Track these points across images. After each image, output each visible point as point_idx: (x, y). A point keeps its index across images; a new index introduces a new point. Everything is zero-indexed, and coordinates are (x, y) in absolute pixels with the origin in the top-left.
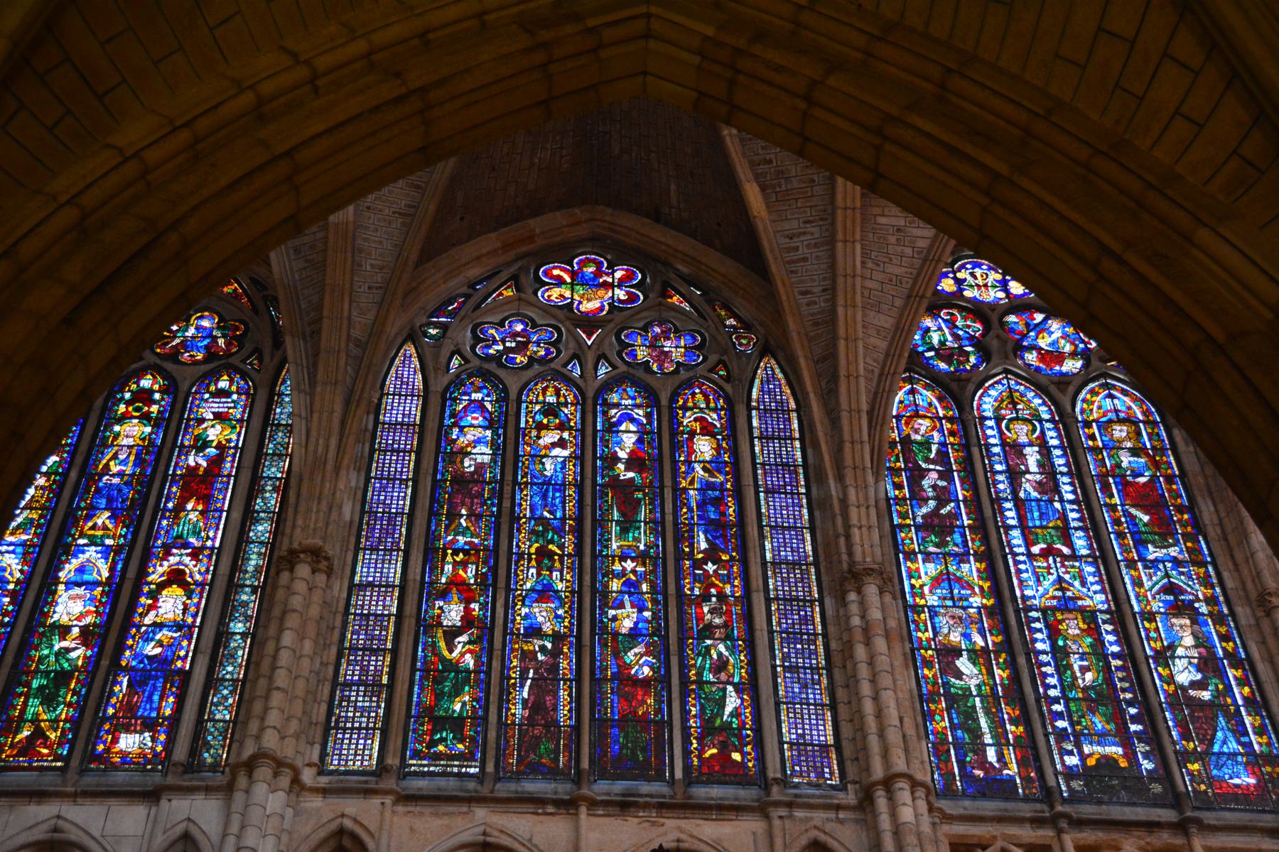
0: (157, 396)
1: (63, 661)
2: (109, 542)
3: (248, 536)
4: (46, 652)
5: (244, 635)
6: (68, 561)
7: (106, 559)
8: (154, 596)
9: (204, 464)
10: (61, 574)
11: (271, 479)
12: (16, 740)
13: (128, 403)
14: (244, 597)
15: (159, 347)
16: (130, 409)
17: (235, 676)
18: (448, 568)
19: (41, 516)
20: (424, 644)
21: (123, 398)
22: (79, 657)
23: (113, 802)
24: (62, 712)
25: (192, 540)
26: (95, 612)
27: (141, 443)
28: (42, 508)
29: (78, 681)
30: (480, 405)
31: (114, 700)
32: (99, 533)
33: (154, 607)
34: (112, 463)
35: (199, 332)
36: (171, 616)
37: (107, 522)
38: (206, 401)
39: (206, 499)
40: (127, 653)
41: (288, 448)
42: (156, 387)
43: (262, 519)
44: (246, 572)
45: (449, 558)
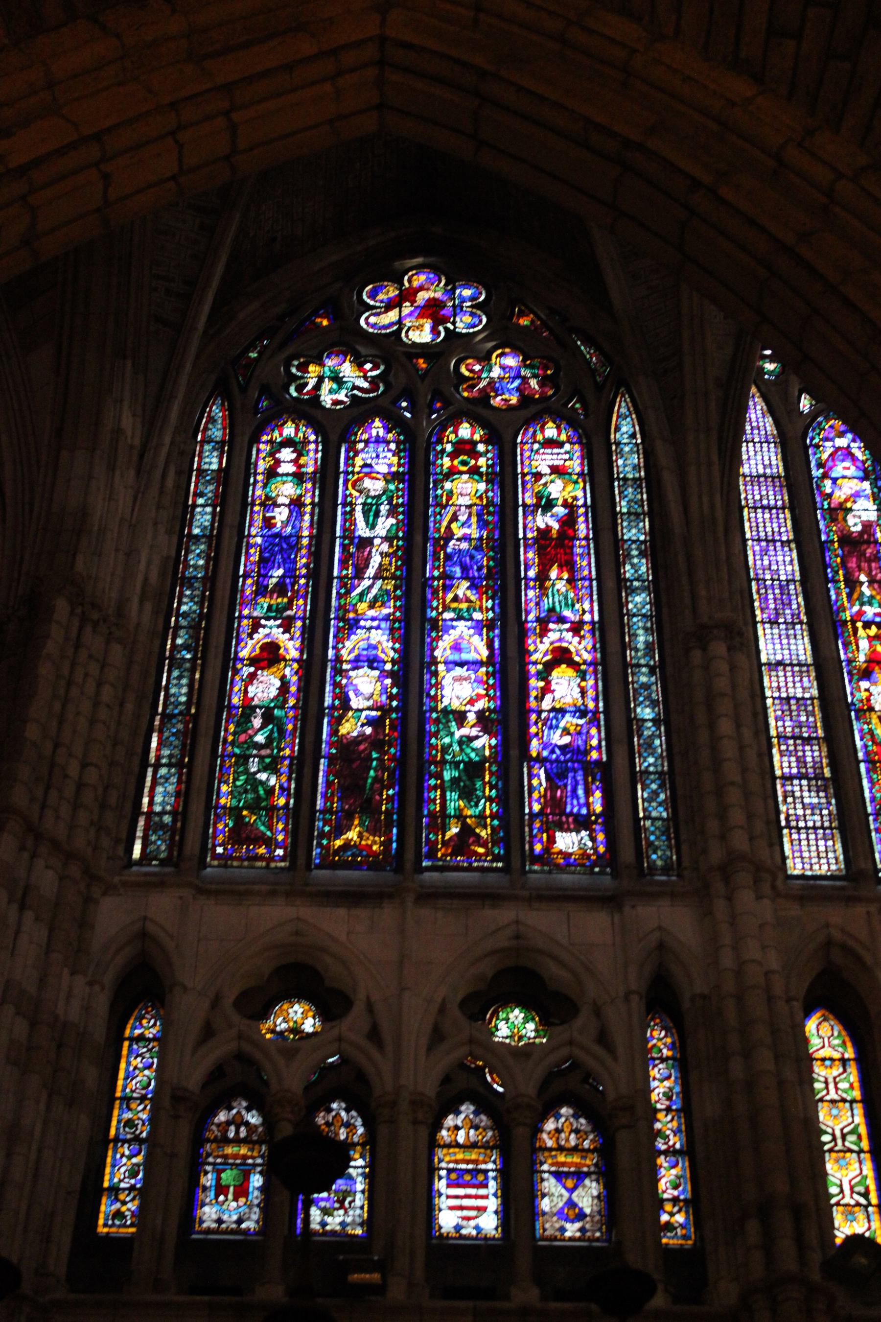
0: (481, 448)
1: (468, 751)
2: (477, 616)
3: (627, 609)
4: (447, 740)
5: (656, 721)
6: (438, 638)
7: (481, 635)
9: (556, 526)
10: (436, 653)
11: (634, 542)
12: (447, 838)
13: (453, 456)
14: (644, 679)
15: (464, 390)
16: (456, 462)
17: (659, 769)
18: (864, 644)
19: (396, 588)
20: (861, 731)
21: (443, 451)
22: (484, 746)
24: (490, 808)
25: (567, 613)
26: (487, 695)
27: (478, 502)
28: (394, 577)
29: (491, 774)
30: (848, 453)
31: (536, 795)
32: (464, 606)
33: (547, 690)
34: (454, 526)
35: (505, 373)
36: (569, 700)
37: (468, 593)
38: (537, 452)
39: (569, 565)
40: (535, 743)
41: (643, 506)
42: (477, 437)
43: (637, 588)
44: (637, 650)
45: (861, 632)
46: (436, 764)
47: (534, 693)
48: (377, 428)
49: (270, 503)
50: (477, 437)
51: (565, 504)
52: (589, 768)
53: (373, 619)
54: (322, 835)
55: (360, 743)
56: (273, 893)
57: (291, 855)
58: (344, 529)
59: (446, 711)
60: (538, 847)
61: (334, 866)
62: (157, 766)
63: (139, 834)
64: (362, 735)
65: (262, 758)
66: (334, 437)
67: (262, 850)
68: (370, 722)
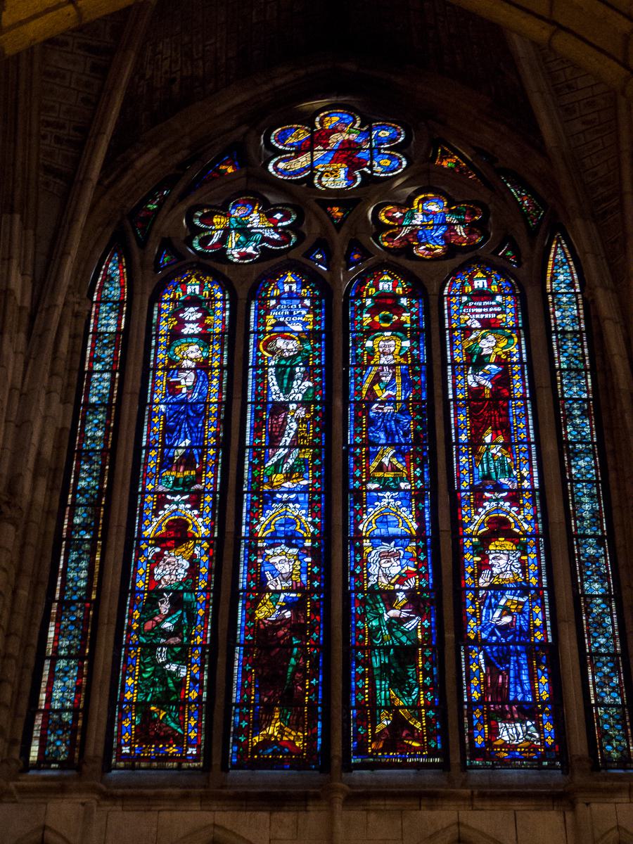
0: (404, 301)
1: (399, 634)
3: (571, 475)
4: (375, 623)
7: (409, 506)
8: (481, 548)
10: (361, 527)
11: (576, 400)
12: (377, 731)
13: (373, 311)
14: (591, 551)
15: (385, 239)
16: (377, 318)
17: (612, 650)
19: (314, 456)
21: (363, 306)
22: (416, 628)
23: (517, 805)
26: (418, 573)
27: (402, 361)
28: (312, 445)
29: (425, 659)
31: (475, 682)
32: (390, 475)
33: (484, 565)
34: (376, 387)
35: (429, 219)
37: (394, 461)
38: (466, 305)
39: (504, 428)
40: (472, 623)
41: (584, 361)
42: (399, 290)
43: (581, 451)
44: (582, 519)
46: (363, 649)
47: (469, 570)
48: (290, 283)
49: (174, 367)
50: (399, 290)
51: (499, 361)
52: (533, 651)
53: (290, 492)
54: (239, 731)
55: (279, 628)
56: (186, 797)
57: (206, 754)
58: (256, 394)
59: (373, 591)
60: (479, 740)
61: (254, 765)
62: (55, 658)
63: (36, 734)
64: (282, 619)
65: (170, 647)
66: (242, 294)
67: (172, 750)
68: (289, 605)
